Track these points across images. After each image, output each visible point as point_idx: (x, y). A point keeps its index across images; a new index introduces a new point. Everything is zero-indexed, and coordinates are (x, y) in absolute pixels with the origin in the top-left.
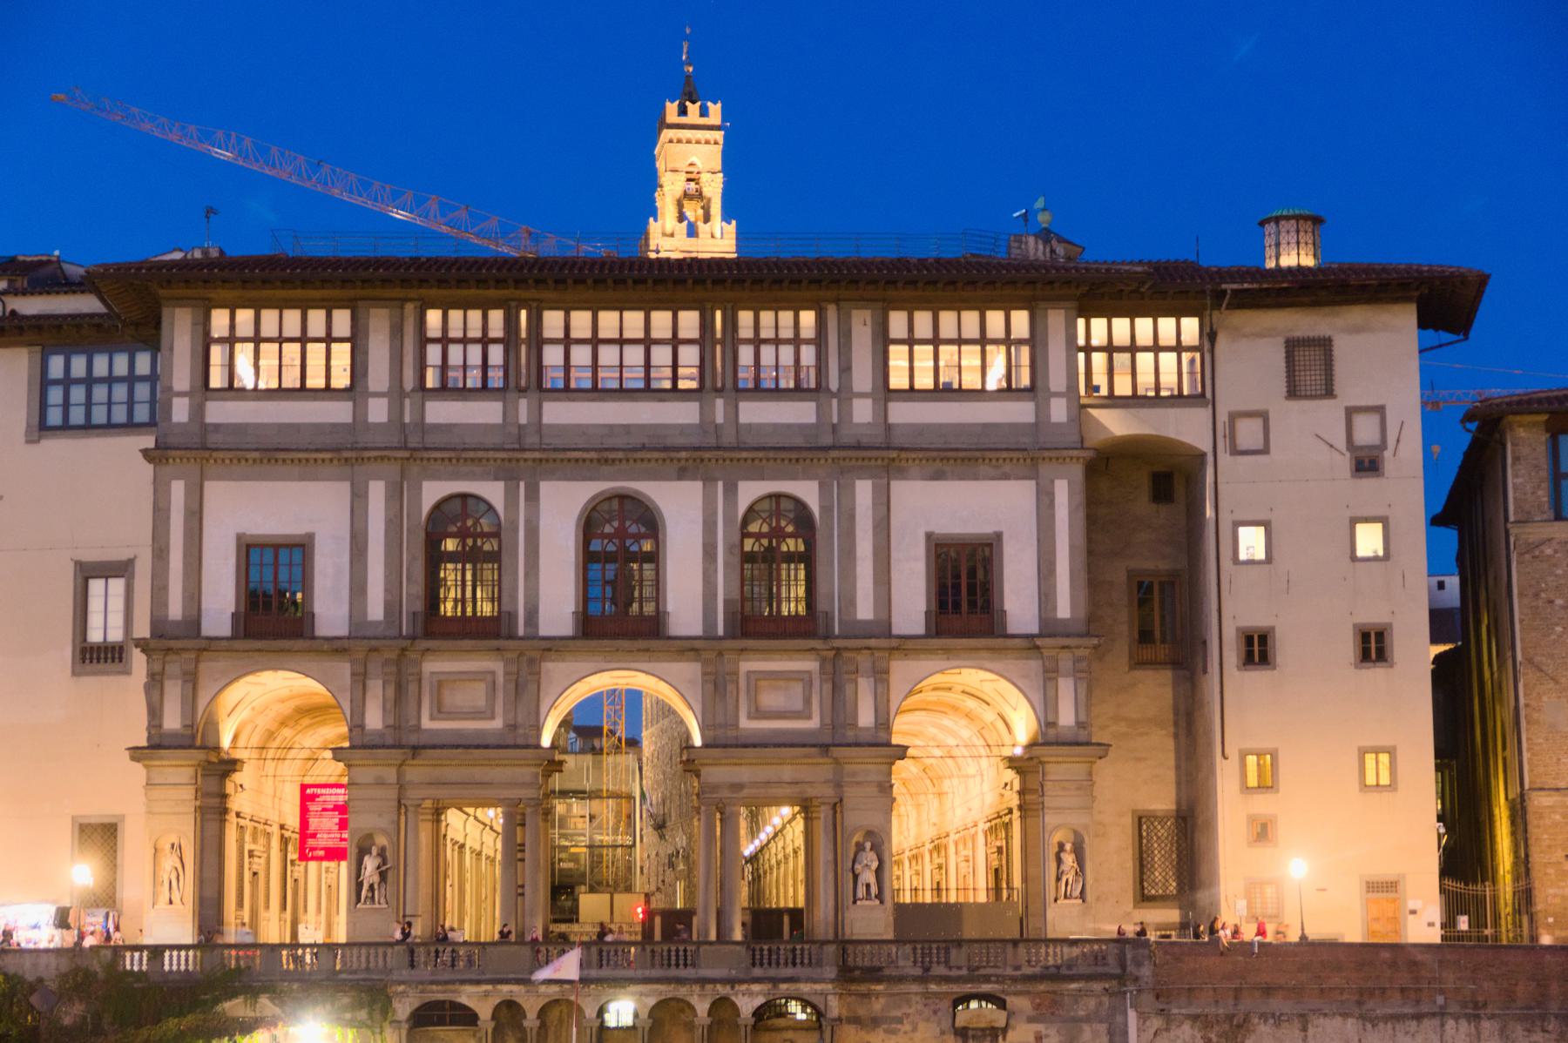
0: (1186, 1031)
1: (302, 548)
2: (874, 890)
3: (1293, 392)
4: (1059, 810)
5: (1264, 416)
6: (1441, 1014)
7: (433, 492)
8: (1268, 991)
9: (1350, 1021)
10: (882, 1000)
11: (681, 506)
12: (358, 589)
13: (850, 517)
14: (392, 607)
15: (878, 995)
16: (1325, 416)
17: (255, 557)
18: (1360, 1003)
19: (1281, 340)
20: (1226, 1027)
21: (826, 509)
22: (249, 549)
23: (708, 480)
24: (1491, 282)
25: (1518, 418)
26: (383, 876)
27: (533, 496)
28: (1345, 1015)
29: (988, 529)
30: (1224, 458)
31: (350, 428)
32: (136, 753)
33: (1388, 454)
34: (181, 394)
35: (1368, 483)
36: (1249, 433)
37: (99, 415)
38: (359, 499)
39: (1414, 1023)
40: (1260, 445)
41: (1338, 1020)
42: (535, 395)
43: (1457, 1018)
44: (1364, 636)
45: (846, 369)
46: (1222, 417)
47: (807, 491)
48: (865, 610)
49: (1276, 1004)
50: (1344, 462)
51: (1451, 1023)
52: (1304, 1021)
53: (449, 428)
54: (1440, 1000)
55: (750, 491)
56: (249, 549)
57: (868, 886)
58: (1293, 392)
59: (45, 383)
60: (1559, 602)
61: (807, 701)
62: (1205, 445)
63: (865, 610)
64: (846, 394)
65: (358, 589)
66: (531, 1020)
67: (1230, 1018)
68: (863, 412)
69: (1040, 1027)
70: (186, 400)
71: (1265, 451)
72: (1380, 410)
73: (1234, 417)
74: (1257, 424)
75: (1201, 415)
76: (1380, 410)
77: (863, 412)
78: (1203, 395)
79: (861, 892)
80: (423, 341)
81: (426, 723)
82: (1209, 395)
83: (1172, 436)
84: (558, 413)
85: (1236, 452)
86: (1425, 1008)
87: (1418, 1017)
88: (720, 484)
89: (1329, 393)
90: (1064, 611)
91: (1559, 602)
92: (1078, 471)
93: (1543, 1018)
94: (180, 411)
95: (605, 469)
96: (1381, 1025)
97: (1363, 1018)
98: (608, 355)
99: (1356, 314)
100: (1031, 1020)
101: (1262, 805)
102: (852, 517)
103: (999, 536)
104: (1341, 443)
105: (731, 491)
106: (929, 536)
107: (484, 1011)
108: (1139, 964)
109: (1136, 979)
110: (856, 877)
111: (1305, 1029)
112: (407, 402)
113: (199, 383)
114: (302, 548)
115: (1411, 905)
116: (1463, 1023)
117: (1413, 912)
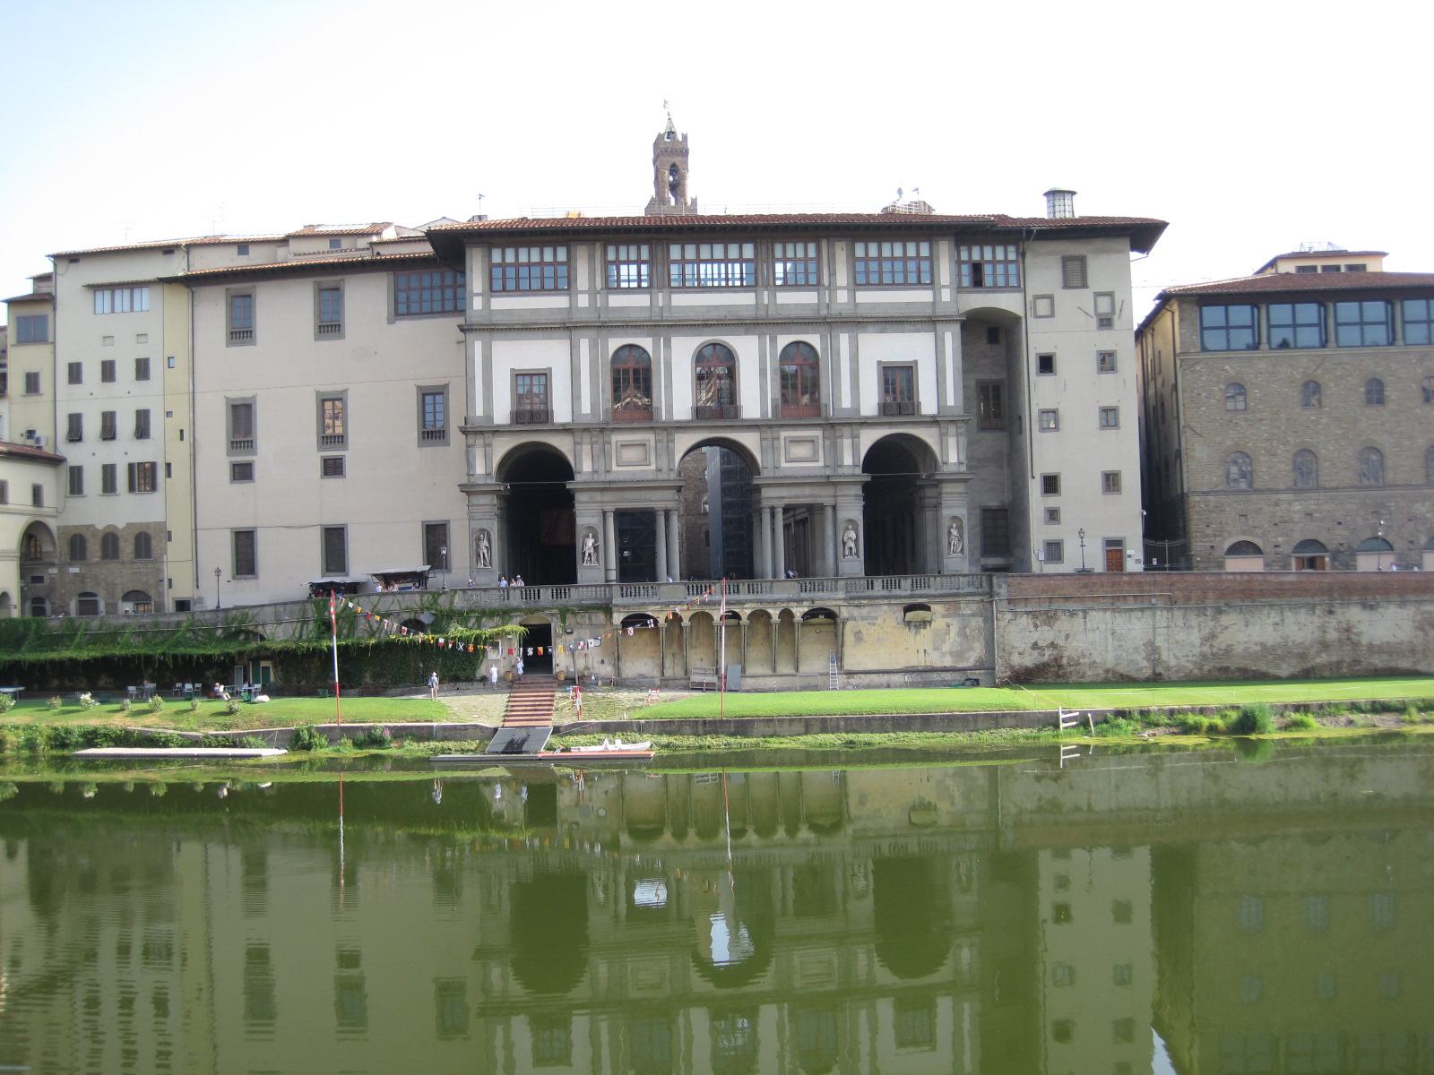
0: (1025, 620)
1: (545, 375)
2: (854, 550)
3: (1066, 286)
4: (950, 507)
5: (1051, 297)
6: (1153, 608)
7: (614, 343)
8: (1066, 599)
9: (1108, 614)
11: (747, 349)
13: (836, 354)
14: (594, 405)
16: (1084, 297)
18: (1113, 604)
19: (1059, 256)
20: (1045, 617)
22: (517, 375)
23: (761, 335)
24: (1168, 227)
26: (596, 548)
27: (668, 345)
29: (911, 359)
30: (1031, 320)
31: (569, 310)
33: (1115, 317)
34: (477, 295)
35: (1105, 333)
36: (1043, 307)
37: (426, 307)
39: (1139, 614)
40: (1048, 313)
41: (1101, 613)
42: (668, 290)
43: (1162, 609)
45: (832, 274)
46: (1030, 298)
47: (814, 339)
49: (1071, 606)
50: (1094, 322)
52: (1085, 612)
55: (784, 340)
56: (517, 375)
57: (851, 548)
59: (397, 291)
60: (1204, 394)
61: (815, 452)
62: (1020, 313)
63: (846, 403)
64: (832, 288)
66: (686, 622)
67: (1046, 612)
68: (842, 297)
69: (949, 620)
70: (480, 298)
71: (1052, 315)
72: (1111, 294)
74: (1047, 302)
75: (1018, 296)
76: (1111, 294)
77: (842, 297)
78: (1019, 286)
79: (847, 552)
82: (1022, 286)
84: (679, 300)
85: (1037, 317)
87: (1142, 610)
88: (768, 337)
89: (1084, 285)
90: (950, 401)
91: (1204, 394)
92: (957, 328)
93: (1205, 608)
94: (477, 304)
95: (707, 330)
97: (1114, 610)
99: (1099, 243)
100: (943, 616)
101: (1052, 501)
102: (839, 354)
103: (916, 362)
104: (1092, 312)
105: (774, 341)
106: (879, 362)
108: (1000, 587)
110: (844, 544)
111: (1085, 618)
112: (598, 296)
113: (487, 288)
114: (545, 375)
115: (1128, 552)
116: (1165, 612)
117: (1130, 556)
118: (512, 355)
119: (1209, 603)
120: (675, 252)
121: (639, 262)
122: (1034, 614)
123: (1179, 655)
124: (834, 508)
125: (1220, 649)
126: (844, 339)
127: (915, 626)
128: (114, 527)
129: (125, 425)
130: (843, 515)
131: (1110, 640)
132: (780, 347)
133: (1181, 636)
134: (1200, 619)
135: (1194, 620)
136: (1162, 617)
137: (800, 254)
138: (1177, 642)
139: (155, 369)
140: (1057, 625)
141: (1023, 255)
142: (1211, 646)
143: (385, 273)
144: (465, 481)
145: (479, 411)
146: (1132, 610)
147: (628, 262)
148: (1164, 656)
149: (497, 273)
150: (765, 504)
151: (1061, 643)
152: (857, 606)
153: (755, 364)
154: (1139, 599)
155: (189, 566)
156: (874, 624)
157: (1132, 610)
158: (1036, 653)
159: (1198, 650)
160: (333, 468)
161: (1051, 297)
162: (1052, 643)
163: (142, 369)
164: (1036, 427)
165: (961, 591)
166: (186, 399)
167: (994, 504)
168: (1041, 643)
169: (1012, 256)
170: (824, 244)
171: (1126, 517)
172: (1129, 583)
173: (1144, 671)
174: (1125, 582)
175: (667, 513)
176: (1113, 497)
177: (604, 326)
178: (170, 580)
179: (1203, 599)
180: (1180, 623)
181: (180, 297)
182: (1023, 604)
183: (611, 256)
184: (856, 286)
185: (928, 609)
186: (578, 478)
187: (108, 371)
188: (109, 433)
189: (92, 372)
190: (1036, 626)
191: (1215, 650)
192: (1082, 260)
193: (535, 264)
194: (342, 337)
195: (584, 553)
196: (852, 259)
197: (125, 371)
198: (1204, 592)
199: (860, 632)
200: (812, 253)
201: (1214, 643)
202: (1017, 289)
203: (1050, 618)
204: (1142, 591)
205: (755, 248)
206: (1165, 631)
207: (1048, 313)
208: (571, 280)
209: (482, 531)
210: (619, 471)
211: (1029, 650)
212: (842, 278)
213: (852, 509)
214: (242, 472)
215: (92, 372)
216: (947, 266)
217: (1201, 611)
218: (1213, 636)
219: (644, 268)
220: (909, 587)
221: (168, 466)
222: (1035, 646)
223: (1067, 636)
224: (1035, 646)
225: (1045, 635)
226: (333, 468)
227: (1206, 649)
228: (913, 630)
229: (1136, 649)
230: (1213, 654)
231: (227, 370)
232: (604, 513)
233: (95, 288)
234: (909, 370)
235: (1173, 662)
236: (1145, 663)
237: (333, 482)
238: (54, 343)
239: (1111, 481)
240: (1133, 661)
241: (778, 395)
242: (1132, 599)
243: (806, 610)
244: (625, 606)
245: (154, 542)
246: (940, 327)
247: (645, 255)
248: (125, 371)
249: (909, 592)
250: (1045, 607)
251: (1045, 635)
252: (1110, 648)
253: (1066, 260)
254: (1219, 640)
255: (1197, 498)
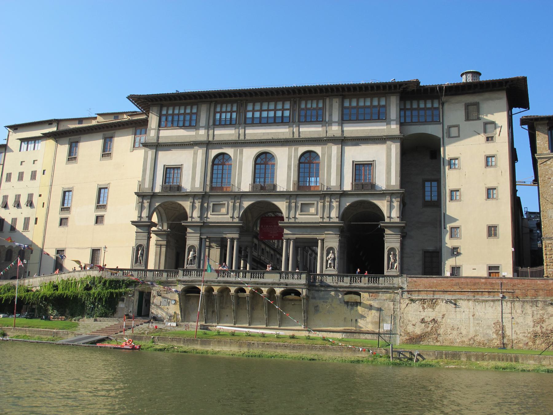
7: (214, 152)
9: (471, 302)
10: (322, 293)
12: (193, 178)
15: (321, 291)
17: (168, 172)
19: (464, 104)
21: (323, 154)
25: (538, 122)
27: (241, 153)
28: (468, 300)
30: (446, 139)
32: (133, 223)
35: (490, 145)
38: (195, 154)
39: (492, 303)
40: (457, 135)
41: (466, 302)
42: (244, 125)
44: (489, 190)
45: (331, 115)
46: (446, 127)
48: (334, 183)
49: (448, 297)
51: (504, 303)
53: (220, 135)
54: (501, 295)
55: (302, 149)
58: (468, 119)
62: (440, 136)
65: (193, 178)
66: (216, 292)
73: (449, 127)
80: (215, 113)
81: (209, 216)
82: (441, 121)
83: (429, 133)
85: (449, 137)
86: (495, 298)
87: (493, 301)
89: (479, 119)
96: (481, 303)
98: (265, 114)
99: (487, 95)
105: (296, 150)
107: (202, 289)
109: (401, 288)
110: (327, 261)
116: (509, 304)
118: (167, 158)
119: (540, 298)
120: (250, 107)
121: (231, 112)
122: (423, 301)
123: (518, 332)
124: (323, 240)
125: (547, 330)
126: (335, 149)
127: (351, 305)
128: (12, 247)
129: (23, 201)
130: (327, 245)
131: (472, 320)
132: (300, 153)
133: (520, 320)
134: (533, 309)
135: (529, 309)
136: (507, 306)
137: (314, 106)
138: (517, 323)
139: (39, 175)
140: (438, 308)
141: (443, 104)
142: (541, 327)
143: (131, 129)
144: (136, 219)
145: (147, 185)
146: (487, 301)
147: (226, 112)
148: (508, 332)
149: (164, 119)
150: (285, 237)
151: (439, 320)
152: (317, 291)
153: (285, 162)
154: (492, 294)
155: (38, 265)
156: (326, 302)
157: (487, 301)
158: (423, 325)
159: (531, 329)
160: (99, 220)
161: (457, 126)
162: (434, 319)
163: (33, 176)
164: (448, 198)
165: (380, 285)
166: (48, 189)
167: (431, 248)
168: (426, 319)
169: (436, 105)
170: (328, 101)
171: (503, 252)
172: (485, 284)
173: (494, 341)
174: (482, 283)
175: (232, 240)
176: (492, 240)
177: (208, 145)
178: (29, 272)
179: (536, 296)
180: (519, 311)
181: (51, 143)
182: (417, 294)
183: (218, 109)
184: (343, 121)
185: (360, 295)
186: (189, 220)
187: (21, 176)
188: (18, 205)
189: (15, 177)
190: (424, 308)
191: (544, 330)
192: (477, 104)
193: (181, 114)
194: (111, 159)
195: (188, 260)
196: (342, 108)
197: (27, 176)
198: (536, 291)
199: (317, 306)
200: (321, 105)
201: (543, 325)
202: (438, 122)
203: (433, 303)
204: (494, 289)
205: (291, 103)
206: (509, 315)
207: (457, 135)
208: (197, 121)
209: (140, 245)
210: (212, 217)
211: (418, 324)
212: (336, 117)
213: (332, 241)
214: (63, 222)
215: (15, 177)
216: (395, 109)
217: (534, 303)
218: (542, 321)
219: (234, 115)
220: (349, 282)
221: (36, 219)
222: (423, 321)
223: (444, 315)
224: (423, 321)
225: (429, 314)
226: (99, 220)
227: (538, 329)
228: (350, 307)
229: (489, 326)
230: (542, 333)
231: (66, 174)
232: (201, 239)
233: (22, 140)
234: (369, 165)
235: (514, 337)
236: (495, 336)
237: (98, 227)
238: (3, 165)
239: (492, 231)
240: (487, 334)
241: (296, 179)
242: (487, 293)
243: (283, 289)
244: (184, 281)
245: (26, 254)
246: (388, 143)
247: (235, 109)
248: (27, 176)
249: (348, 284)
250: (430, 296)
251: (429, 314)
252: (472, 325)
253: (467, 106)
254: (547, 323)
255: (548, 242)
